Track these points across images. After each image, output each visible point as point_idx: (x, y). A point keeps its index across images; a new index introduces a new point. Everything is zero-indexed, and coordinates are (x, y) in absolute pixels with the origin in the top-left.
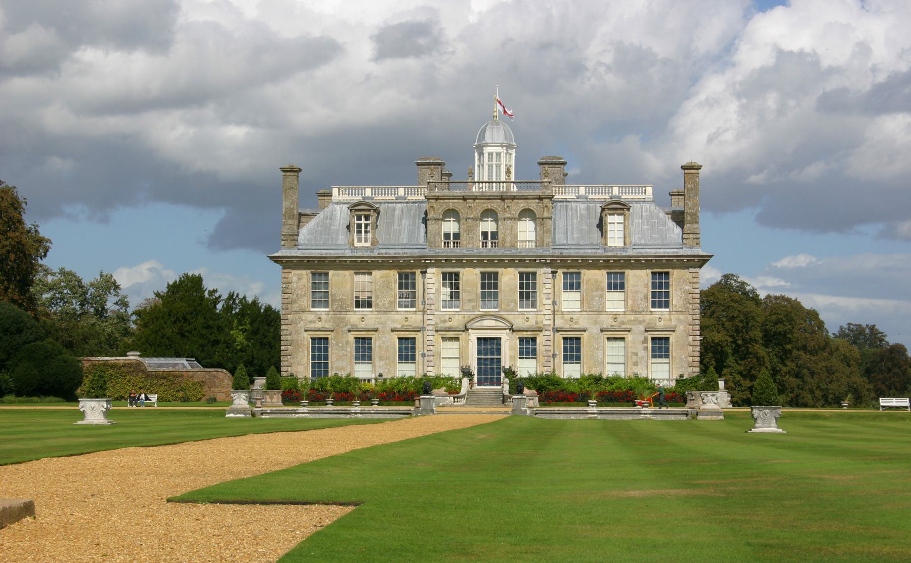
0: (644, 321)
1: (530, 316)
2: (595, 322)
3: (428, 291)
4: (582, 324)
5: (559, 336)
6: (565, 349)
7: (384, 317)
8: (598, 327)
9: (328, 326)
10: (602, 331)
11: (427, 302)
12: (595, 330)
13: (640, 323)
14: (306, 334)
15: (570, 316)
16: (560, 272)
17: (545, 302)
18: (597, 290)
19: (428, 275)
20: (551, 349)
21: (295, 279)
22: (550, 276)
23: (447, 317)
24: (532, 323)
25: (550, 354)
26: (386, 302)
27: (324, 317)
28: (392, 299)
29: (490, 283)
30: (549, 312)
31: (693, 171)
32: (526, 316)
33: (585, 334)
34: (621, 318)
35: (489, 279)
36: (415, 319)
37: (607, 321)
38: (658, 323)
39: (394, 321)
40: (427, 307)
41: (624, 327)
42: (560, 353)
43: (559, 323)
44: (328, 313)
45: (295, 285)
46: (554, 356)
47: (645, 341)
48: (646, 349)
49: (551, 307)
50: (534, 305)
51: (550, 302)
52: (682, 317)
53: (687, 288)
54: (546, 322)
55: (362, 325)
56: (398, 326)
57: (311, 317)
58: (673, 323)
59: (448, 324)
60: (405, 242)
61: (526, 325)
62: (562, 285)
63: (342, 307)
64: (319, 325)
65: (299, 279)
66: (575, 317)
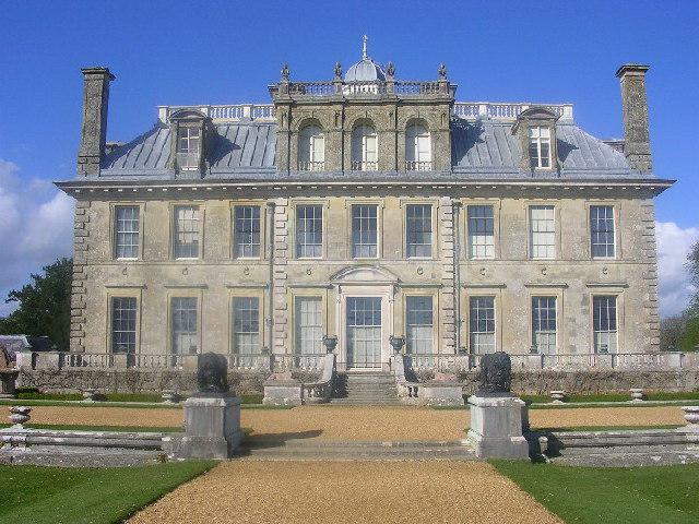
0: (583, 273)
2: (516, 275)
3: (276, 231)
4: (499, 278)
6: (472, 313)
9: (137, 281)
11: (276, 246)
12: (515, 286)
13: (578, 276)
14: (105, 292)
15: (480, 266)
16: (466, 201)
19: (277, 209)
21: (94, 216)
23: (304, 269)
24: (427, 274)
27: (131, 269)
29: (363, 222)
31: (635, 73)
34: (551, 270)
35: (365, 214)
36: (259, 271)
37: (531, 272)
38: (602, 276)
40: (276, 253)
41: (555, 282)
43: (465, 276)
44: (135, 264)
45: (93, 224)
47: (585, 301)
48: (585, 312)
50: (427, 252)
51: (451, 245)
52: (633, 267)
53: (639, 227)
55: (184, 280)
56: (235, 283)
57: (113, 269)
58: (622, 276)
59: (306, 279)
61: (417, 279)
63: (156, 255)
64: (123, 281)
65: (99, 216)
66: (487, 267)
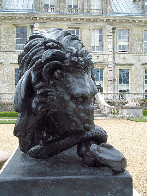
1: (99, 56)
2: (139, 60)
5: (117, 68)
6: (120, 78)
7: (6, 55)
8: (140, 63)
10: (142, 65)
12: (138, 65)
17: (109, 47)
18: (139, 41)
19: (35, 29)
20: (112, 76)
22: (111, 31)
25: (112, 79)
26: (8, 46)
28: (11, 44)
30: (112, 53)
32: (97, 56)
33: (133, 67)
39: (12, 58)
42: (117, 78)
43: (117, 60)
46: (114, 80)
49: (112, 50)
51: (111, 47)
54: (109, 59)
60: (21, 8)
62: (118, 37)
